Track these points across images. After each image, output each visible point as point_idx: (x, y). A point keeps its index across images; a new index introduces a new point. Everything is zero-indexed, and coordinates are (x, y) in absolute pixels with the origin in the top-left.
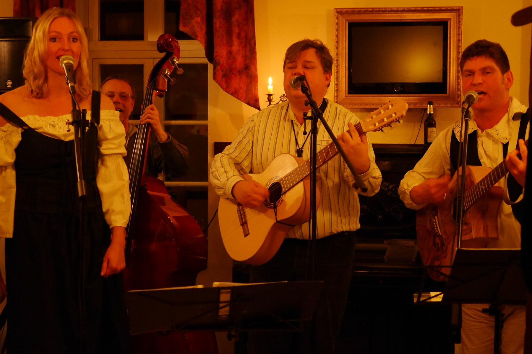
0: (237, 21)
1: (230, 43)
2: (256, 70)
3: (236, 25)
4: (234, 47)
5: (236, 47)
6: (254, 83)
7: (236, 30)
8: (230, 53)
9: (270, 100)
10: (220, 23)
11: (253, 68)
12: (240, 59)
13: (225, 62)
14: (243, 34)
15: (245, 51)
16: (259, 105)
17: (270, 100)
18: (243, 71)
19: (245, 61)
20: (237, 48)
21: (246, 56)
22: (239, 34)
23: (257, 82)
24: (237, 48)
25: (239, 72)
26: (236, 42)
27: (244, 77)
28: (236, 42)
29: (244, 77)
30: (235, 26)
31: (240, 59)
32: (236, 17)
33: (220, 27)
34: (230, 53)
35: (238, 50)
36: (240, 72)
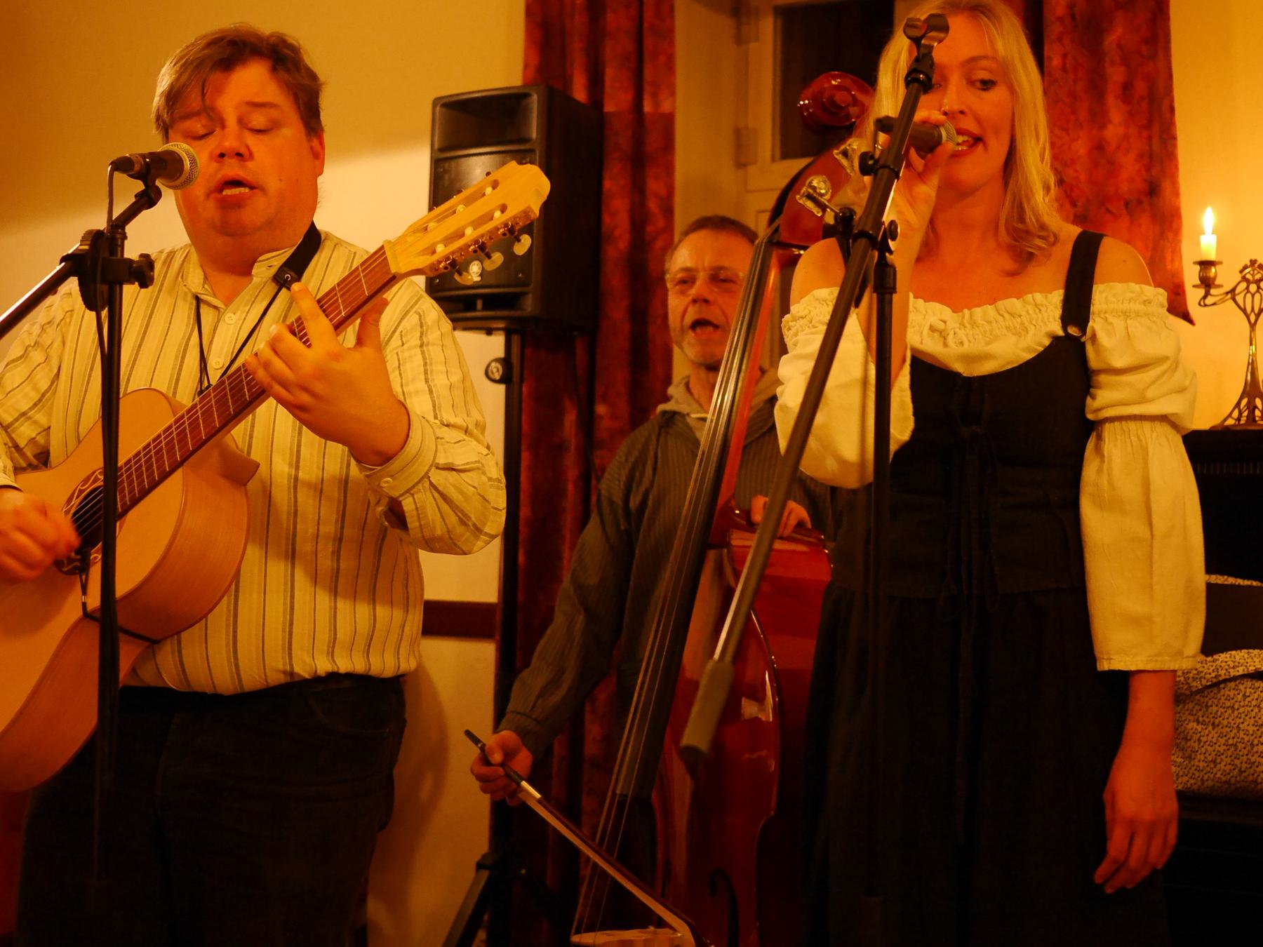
0: (1119, 46)
1: (1099, 118)
2: (1177, 193)
3: (1118, 60)
4: (1110, 127)
5: (1115, 129)
6: (1170, 235)
7: (1116, 75)
8: (1099, 147)
9: (1207, 283)
10: (1065, 56)
11: (1166, 185)
12: (1129, 166)
13: (1083, 177)
14: (1141, 87)
15: (1150, 138)
16: (1185, 304)
17: (1207, 283)
18: (1140, 202)
19: (1148, 170)
20: (1121, 130)
21: (1151, 156)
22: (1127, 87)
23: (1177, 232)
24: (1121, 130)
25: (1127, 204)
26: (1116, 112)
27: (1144, 219)
28: (1116, 112)
29: (1144, 219)
30: (1112, 63)
31: (1129, 166)
32: (1117, 34)
33: (1064, 69)
34: (1099, 147)
35: (1126, 137)
36: (1132, 207)
